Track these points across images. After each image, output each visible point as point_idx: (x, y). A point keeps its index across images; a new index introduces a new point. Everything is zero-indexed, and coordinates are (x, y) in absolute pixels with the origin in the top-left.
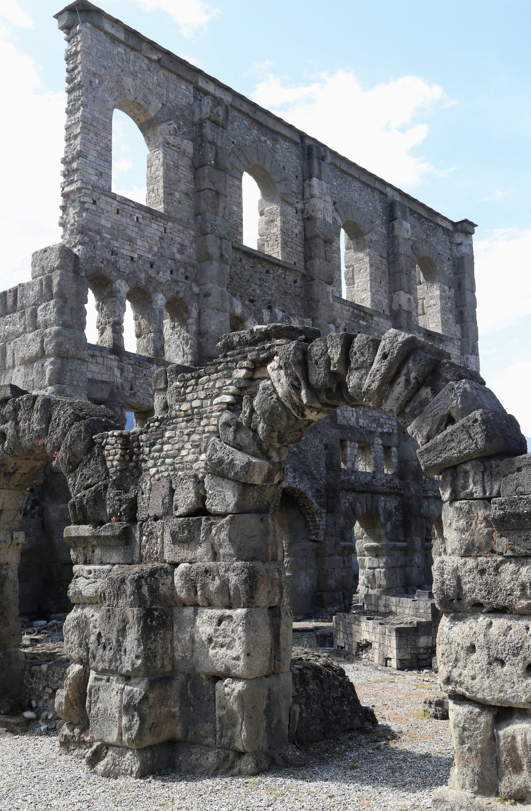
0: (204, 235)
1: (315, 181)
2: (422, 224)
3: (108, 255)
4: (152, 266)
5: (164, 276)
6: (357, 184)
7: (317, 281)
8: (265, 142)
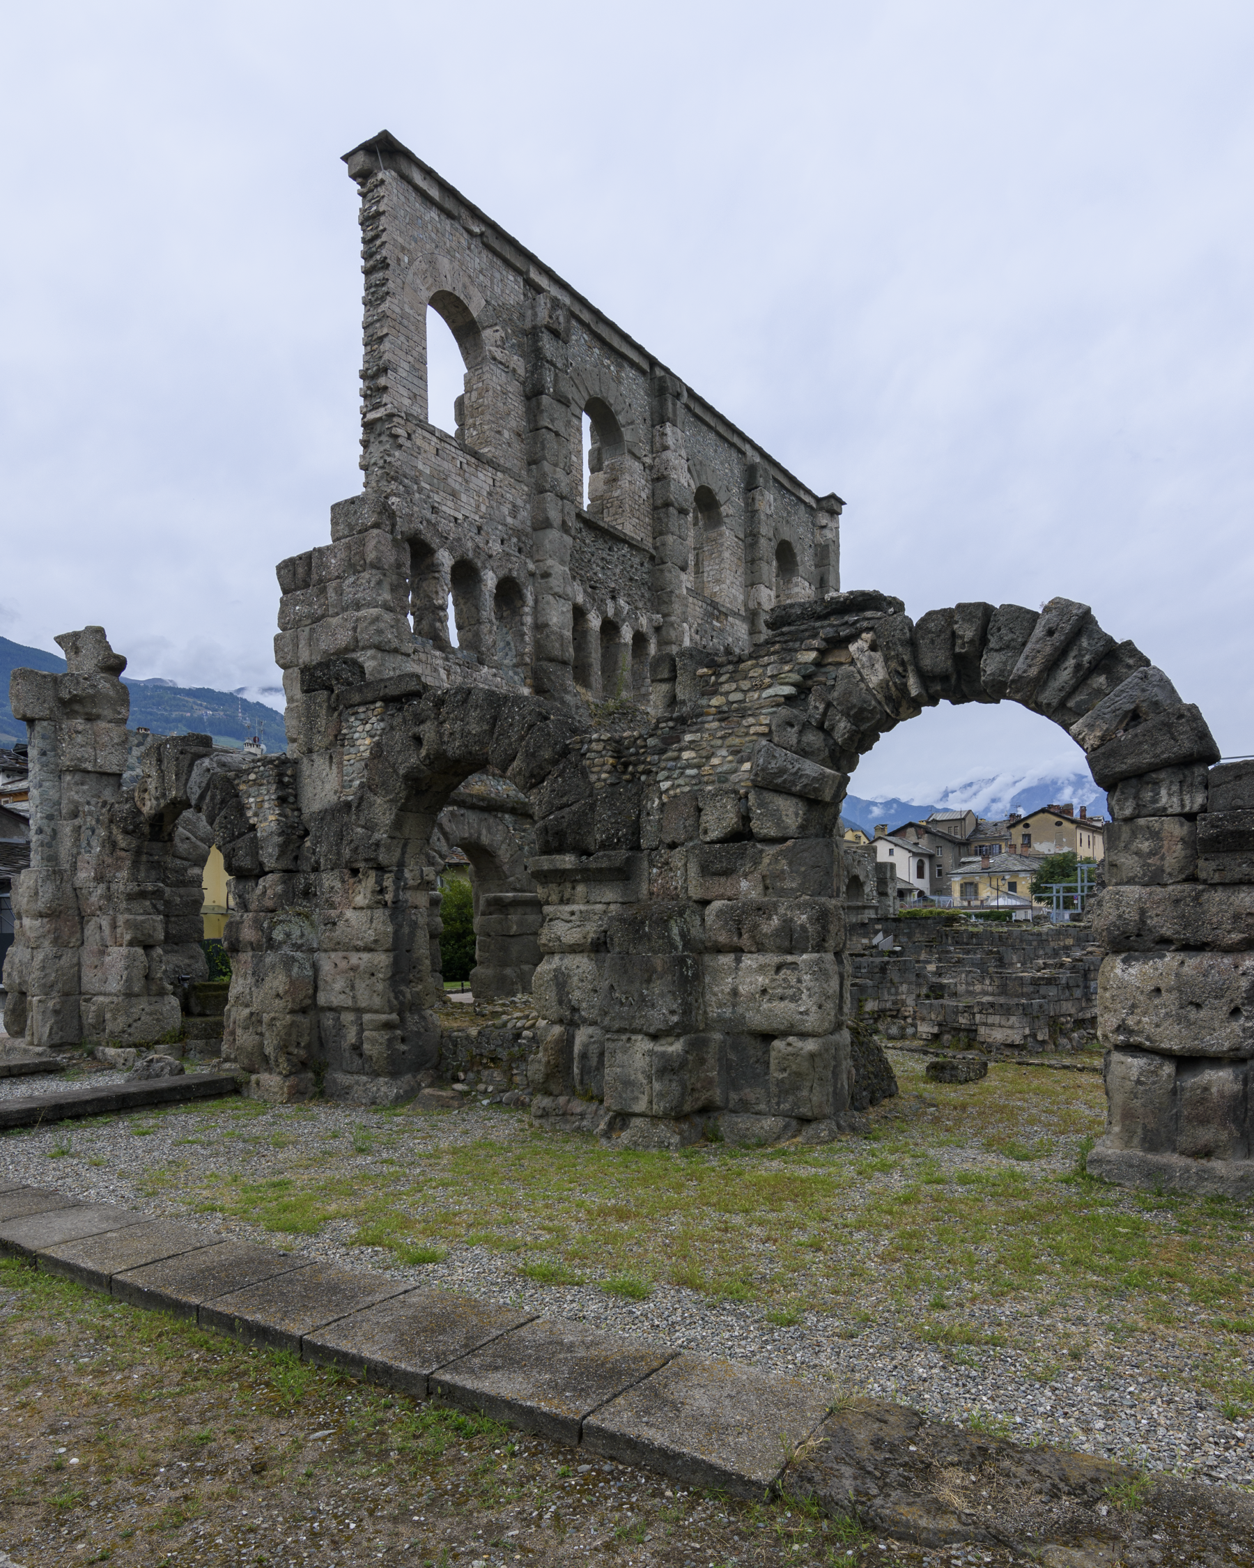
0: (541, 492)
1: (668, 428)
2: (783, 497)
3: (428, 513)
4: (479, 529)
5: (496, 548)
6: (712, 436)
7: (670, 564)
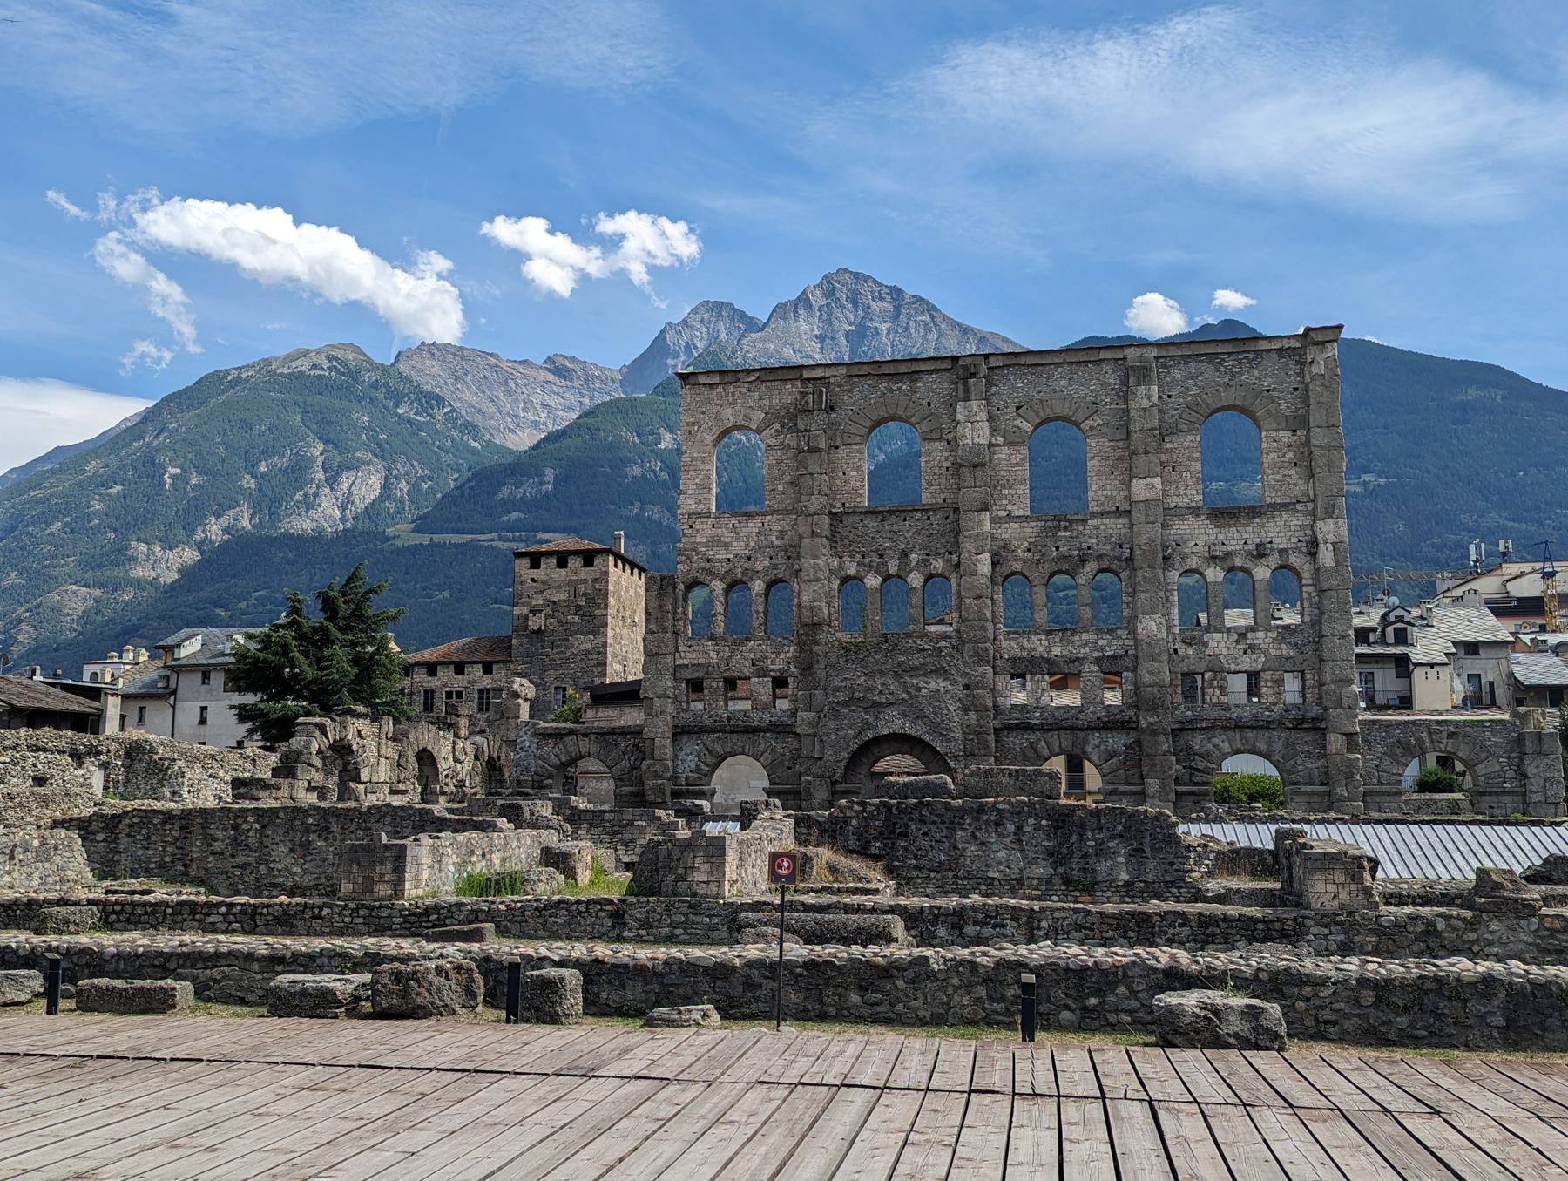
1: (960, 407)
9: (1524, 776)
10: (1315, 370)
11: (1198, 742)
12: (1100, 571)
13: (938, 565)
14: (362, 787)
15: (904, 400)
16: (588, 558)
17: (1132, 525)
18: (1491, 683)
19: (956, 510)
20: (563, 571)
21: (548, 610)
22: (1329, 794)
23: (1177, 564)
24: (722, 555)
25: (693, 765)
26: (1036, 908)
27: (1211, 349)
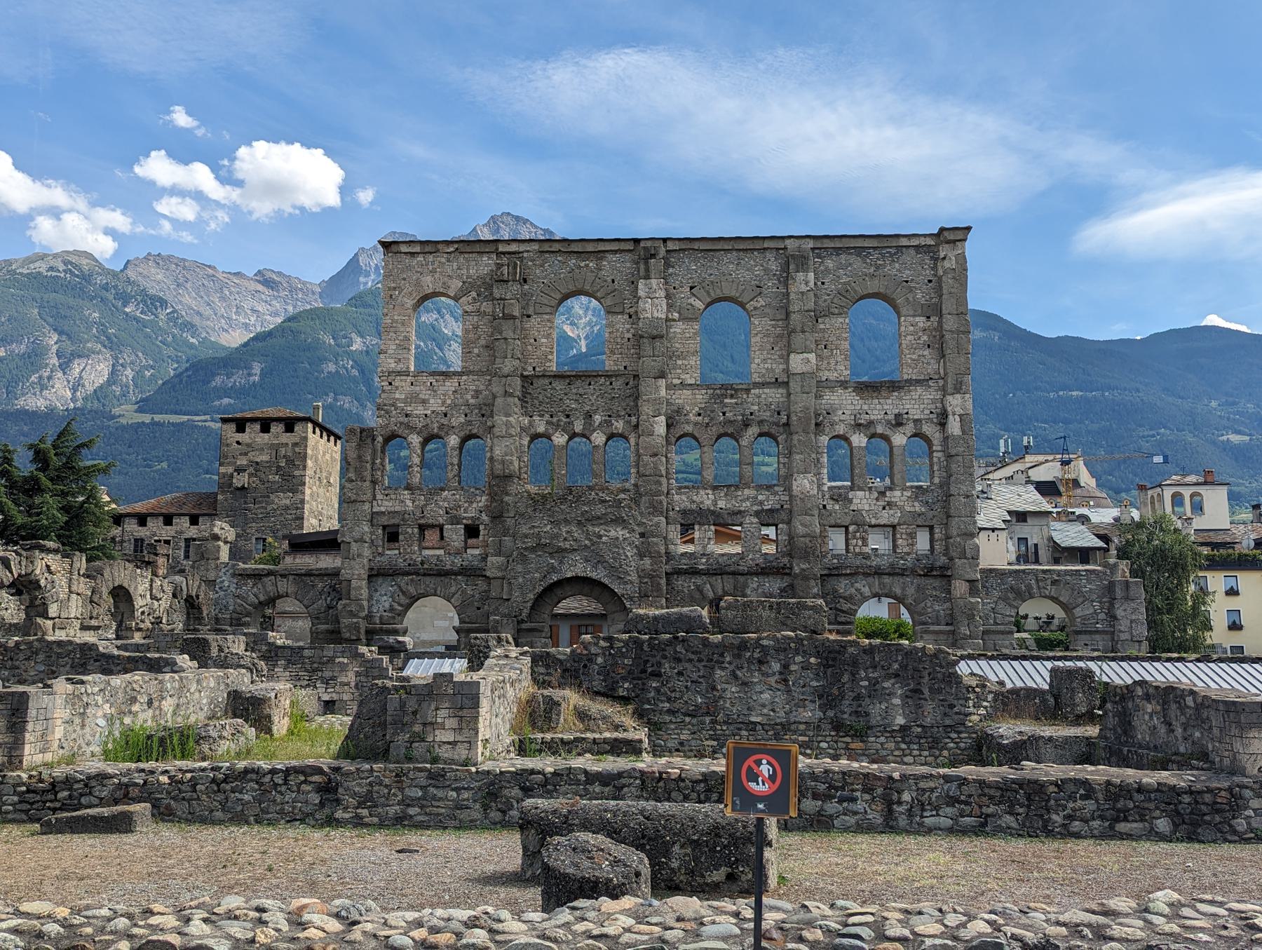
1: (641, 284)
8: (587, 266)
9: (1114, 618)
10: (947, 264)
11: (842, 586)
12: (761, 435)
13: (619, 425)
14: (49, 623)
15: (590, 277)
16: (290, 424)
17: (789, 394)
18: (1036, 545)
19: (636, 377)
20: (266, 436)
21: (251, 470)
22: (953, 632)
23: (827, 430)
24: (420, 410)
25: (387, 605)
26: (896, 775)
27: (859, 243)
